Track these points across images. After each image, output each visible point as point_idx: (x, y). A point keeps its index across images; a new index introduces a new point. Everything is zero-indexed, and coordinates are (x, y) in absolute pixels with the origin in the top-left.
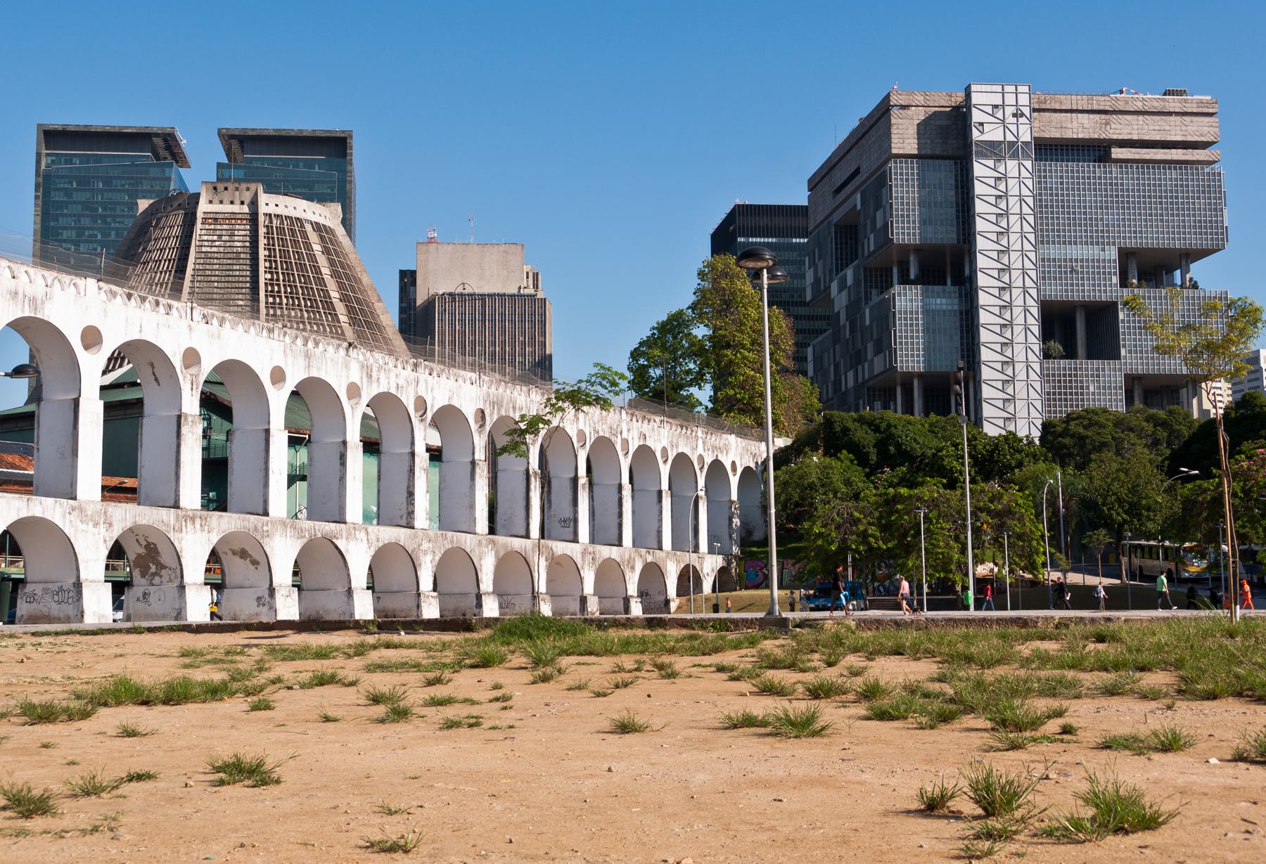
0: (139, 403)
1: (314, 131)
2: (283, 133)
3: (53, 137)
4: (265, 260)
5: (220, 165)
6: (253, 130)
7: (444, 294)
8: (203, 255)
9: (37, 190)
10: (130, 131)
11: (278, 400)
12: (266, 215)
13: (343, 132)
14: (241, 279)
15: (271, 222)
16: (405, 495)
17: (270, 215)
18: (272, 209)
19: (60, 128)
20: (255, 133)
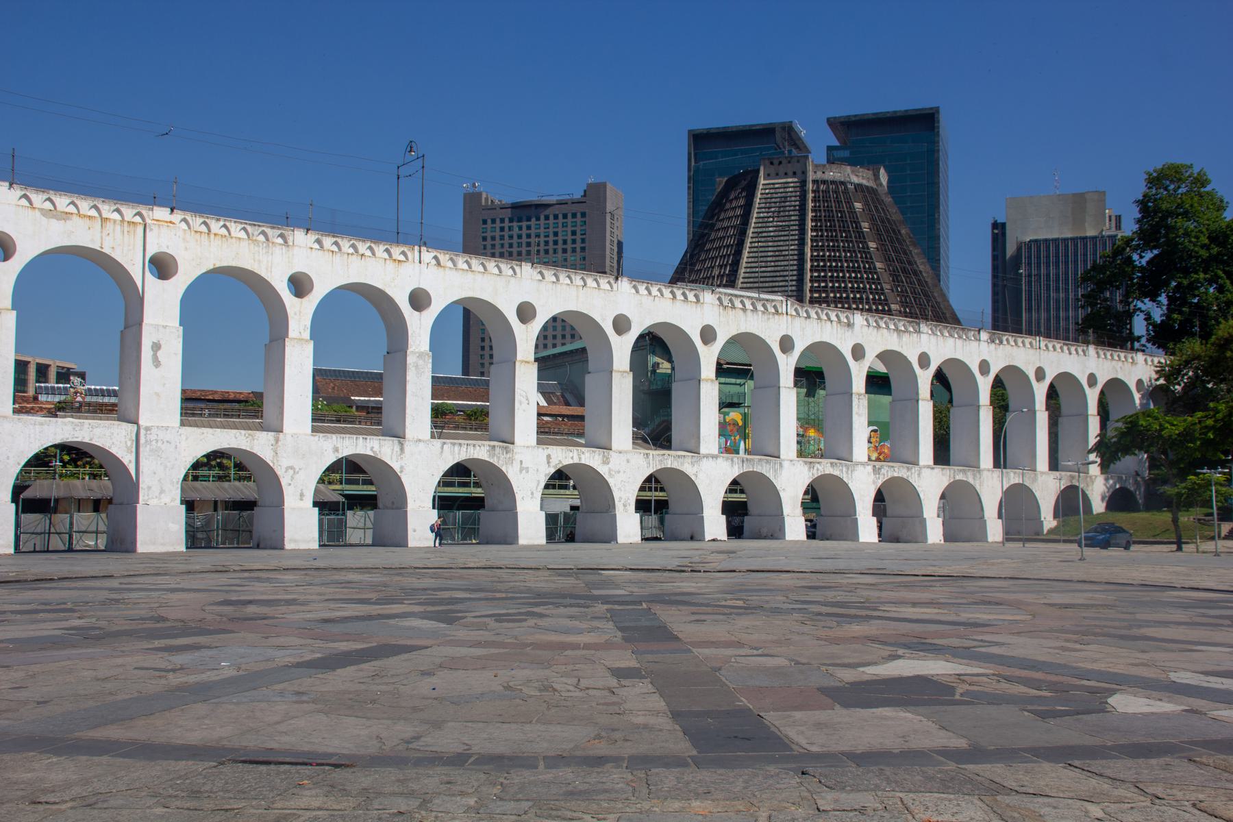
0: (584, 350)
1: (906, 111)
2: (880, 116)
3: (701, 141)
4: (812, 220)
5: (830, 149)
6: (856, 116)
7: (1030, 241)
8: (761, 220)
9: (689, 182)
10: (758, 128)
11: (622, 349)
12: (814, 182)
13: (931, 109)
14: (782, 238)
15: (818, 187)
16: (620, 449)
17: (817, 181)
18: (819, 175)
19: (705, 132)
20: (857, 118)
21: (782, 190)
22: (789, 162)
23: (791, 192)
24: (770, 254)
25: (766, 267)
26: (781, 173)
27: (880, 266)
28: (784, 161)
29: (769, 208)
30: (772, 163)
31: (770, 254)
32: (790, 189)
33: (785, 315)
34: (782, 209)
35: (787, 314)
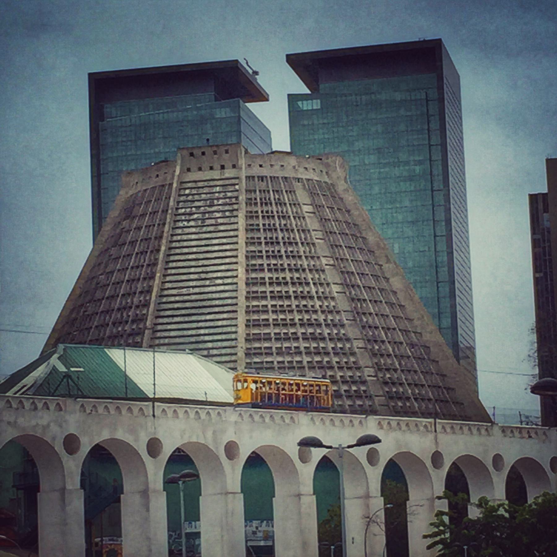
5: (293, 99)
21: (206, 190)
22: (215, 153)
23: (219, 192)
24: (192, 277)
25: (189, 295)
26: (206, 166)
27: (339, 290)
28: (208, 151)
29: (191, 214)
30: (192, 154)
31: (192, 277)
32: (218, 189)
33: (152, 417)
34: (207, 215)
35: (154, 416)
